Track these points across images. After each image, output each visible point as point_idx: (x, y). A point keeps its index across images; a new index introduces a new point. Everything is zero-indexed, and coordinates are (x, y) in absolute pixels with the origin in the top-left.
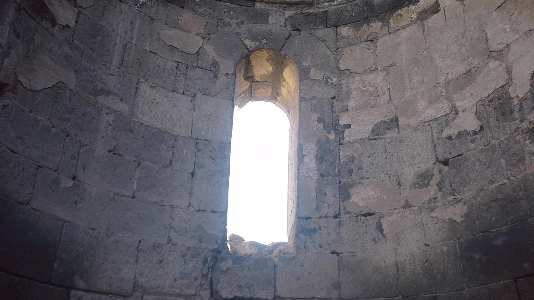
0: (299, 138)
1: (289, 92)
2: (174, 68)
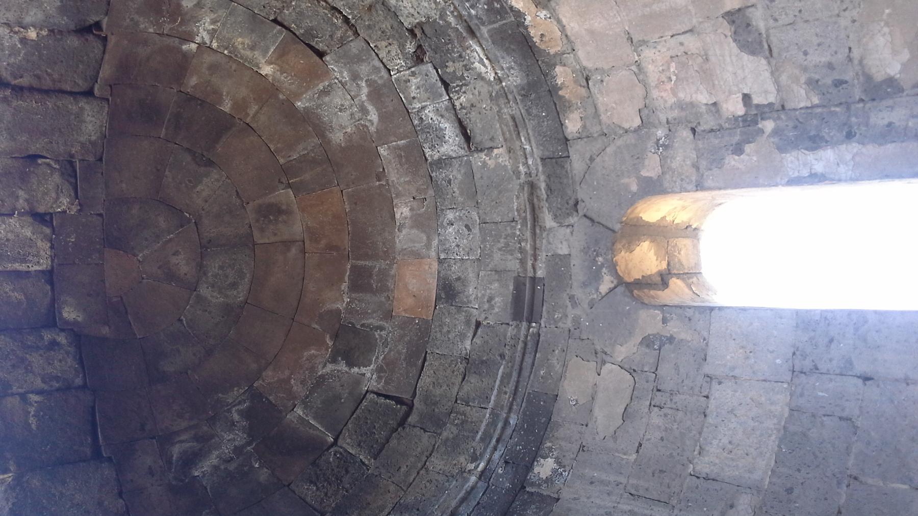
0: (776, 185)
1: (684, 208)
2: (661, 413)
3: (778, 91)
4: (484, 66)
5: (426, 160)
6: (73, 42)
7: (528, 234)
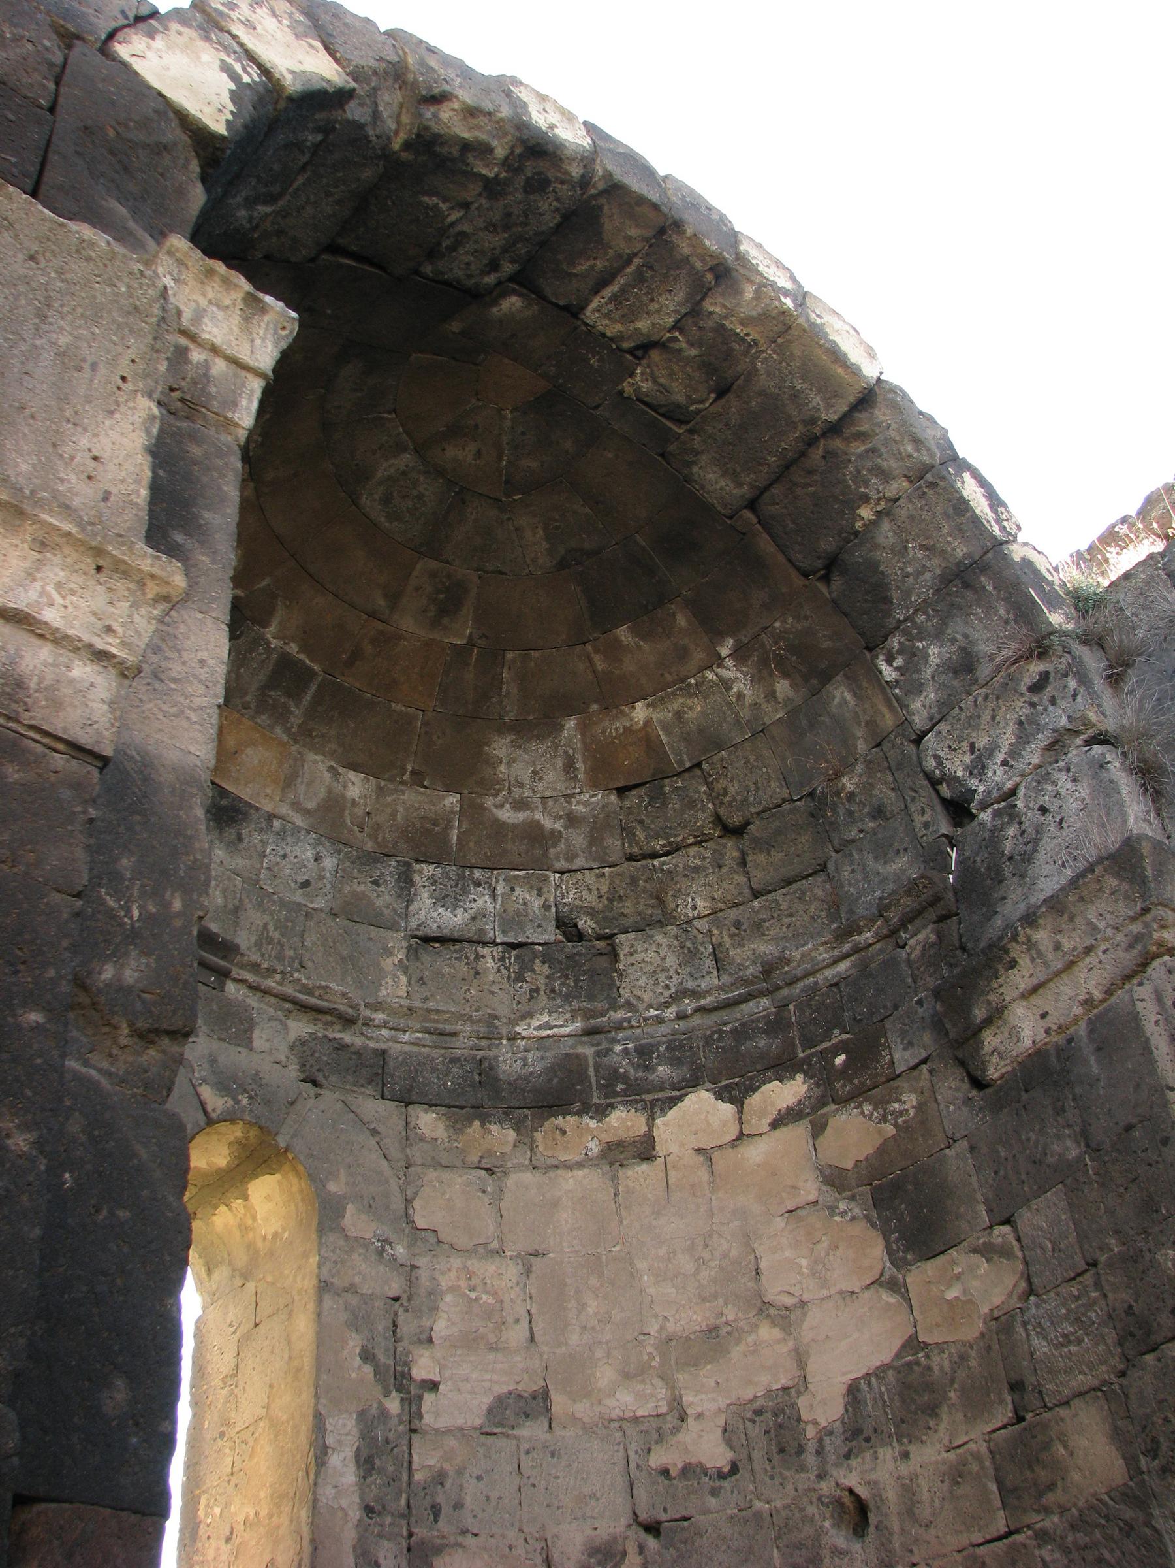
1: (243, 1228)
3: (436, 1430)
4: (539, 1028)
5: (418, 861)
6: (827, 544)
7: (289, 990)
